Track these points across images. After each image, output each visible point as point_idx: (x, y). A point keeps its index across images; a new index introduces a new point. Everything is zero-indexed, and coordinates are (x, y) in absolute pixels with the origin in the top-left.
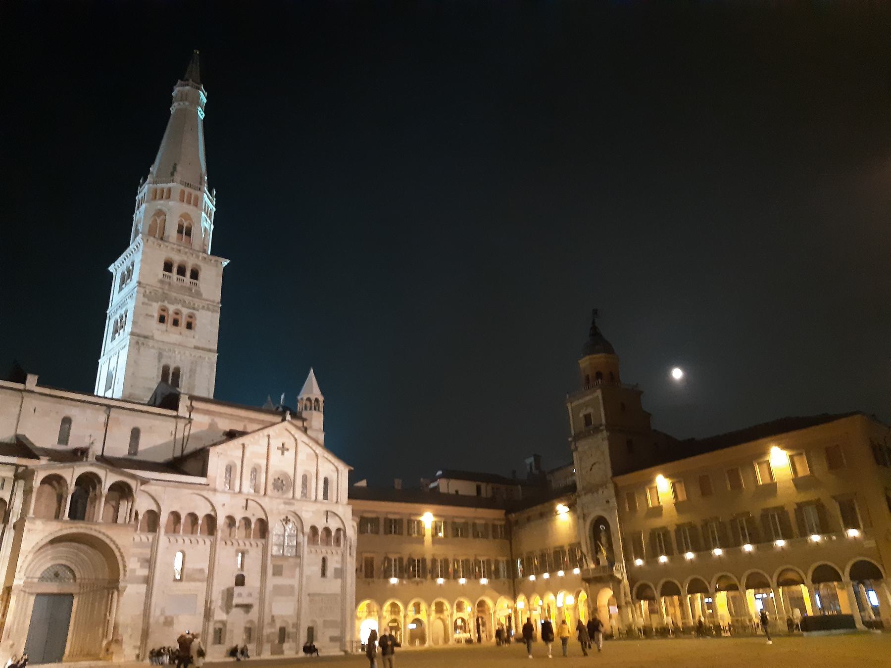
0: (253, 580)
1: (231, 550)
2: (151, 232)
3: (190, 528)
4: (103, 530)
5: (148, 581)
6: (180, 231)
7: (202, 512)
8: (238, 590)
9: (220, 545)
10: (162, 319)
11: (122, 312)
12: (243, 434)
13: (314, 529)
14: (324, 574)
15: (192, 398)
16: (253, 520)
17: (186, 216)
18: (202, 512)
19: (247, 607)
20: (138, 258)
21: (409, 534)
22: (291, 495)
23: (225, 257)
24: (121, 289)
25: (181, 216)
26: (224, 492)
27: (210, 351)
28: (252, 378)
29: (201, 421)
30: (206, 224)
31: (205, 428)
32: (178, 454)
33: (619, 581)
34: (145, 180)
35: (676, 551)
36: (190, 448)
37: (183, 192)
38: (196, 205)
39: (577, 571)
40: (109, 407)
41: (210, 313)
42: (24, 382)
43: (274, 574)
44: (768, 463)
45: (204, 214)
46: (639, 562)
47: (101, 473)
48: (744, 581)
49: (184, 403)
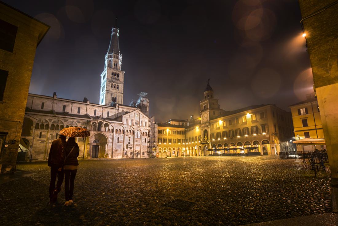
0: (132, 143)
1: (128, 137)
2: (108, 67)
3: (119, 132)
4: (104, 133)
5: (112, 143)
6: (115, 65)
7: (122, 129)
8: (129, 145)
9: (125, 136)
10: (112, 87)
11: (104, 85)
12: (129, 112)
13: (144, 133)
14: (146, 142)
15: (119, 105)
16: (132, 131)
17: (116, 61)
18: (122, 129)
19: (131, 148)
20: (106, 72)
21: (164, 133)
22: (139, 126)
23: (124, 71)
24: (103, 80)
25: (115, 61)
26: (126, 125)
27: (122, 93)
28: (130, 100)
29: (121, 110)
30: (120, 63)
31: (122, 111)
32: (116, 117)
33: (209, 144)
34: (107, 53)
35: (222, 138)
36: (118, 116)
37: (115, 56)
38: (118, 59)
39: (200, 142)
40: (103, 107)
41: (121, 85)
42: (87, 103)
43: (136, 142)
44: (246, 117)
45: (119, 61)
46: (214, 140)
47: (103, 121)
48: (237, 144)
49: (117, 105)
